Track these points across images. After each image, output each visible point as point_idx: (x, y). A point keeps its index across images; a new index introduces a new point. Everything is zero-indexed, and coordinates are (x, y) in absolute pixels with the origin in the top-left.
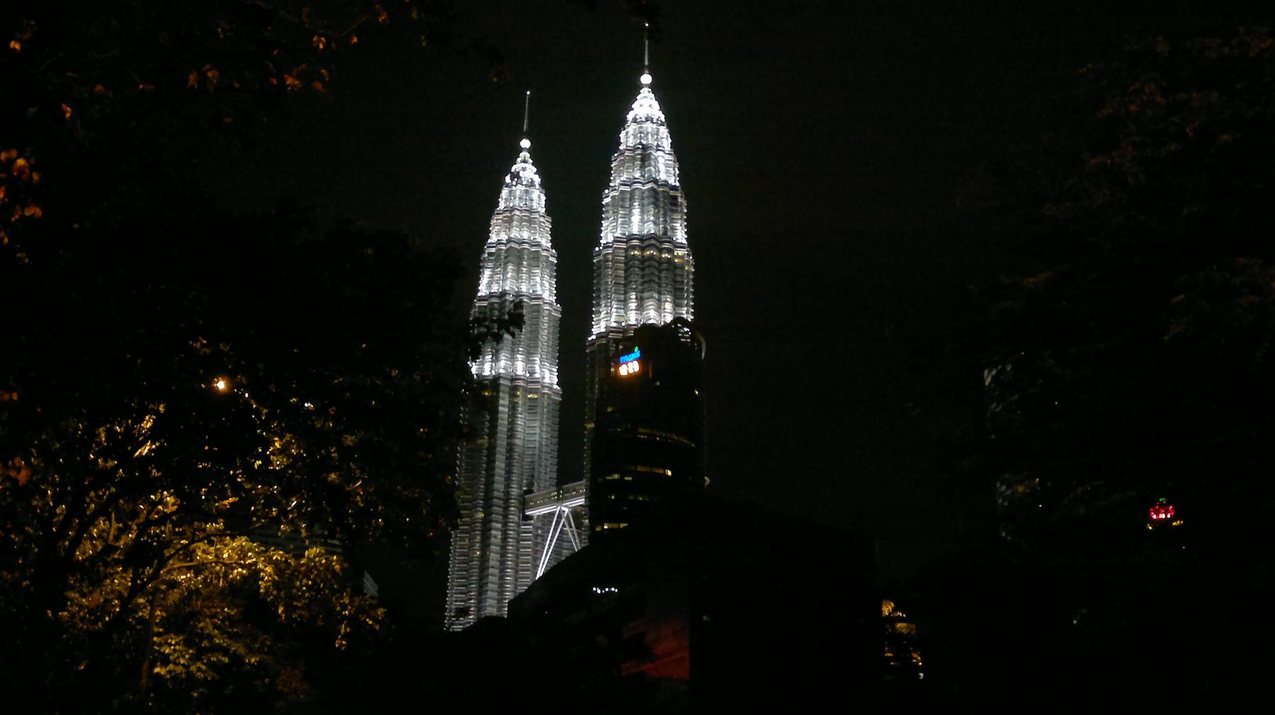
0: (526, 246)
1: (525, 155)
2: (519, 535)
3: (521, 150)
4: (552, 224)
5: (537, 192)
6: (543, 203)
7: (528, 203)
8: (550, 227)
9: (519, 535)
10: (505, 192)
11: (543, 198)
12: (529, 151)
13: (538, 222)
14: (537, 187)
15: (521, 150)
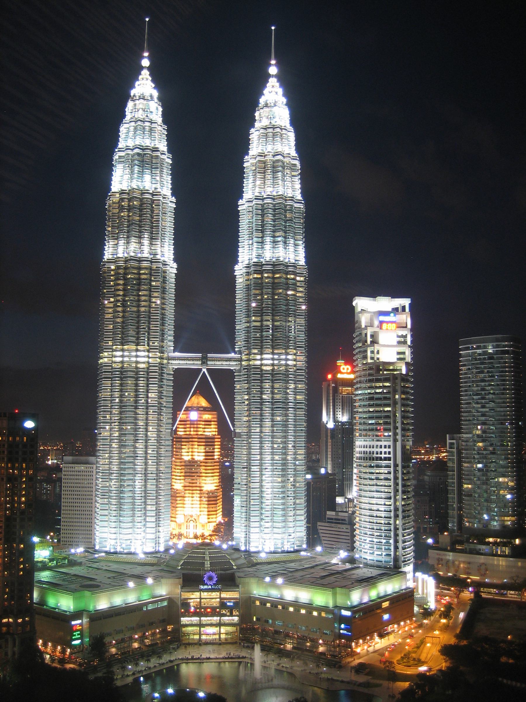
0: (149, 152)
1: (145, 74)
2: (148, 375)
3: (142, 68)
4: (167, 131)
5: (156, 105)
6: (160, 113)
7: (148, 115)
8: (166, 133)
9: (148, 375)
10: (130, 105)
11: (160, 109)
12: (149, 68)
13: (157, 132)
14: (156, 100)
15: (142, 68)
